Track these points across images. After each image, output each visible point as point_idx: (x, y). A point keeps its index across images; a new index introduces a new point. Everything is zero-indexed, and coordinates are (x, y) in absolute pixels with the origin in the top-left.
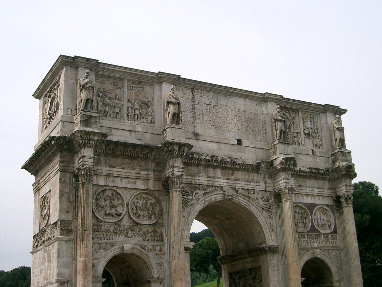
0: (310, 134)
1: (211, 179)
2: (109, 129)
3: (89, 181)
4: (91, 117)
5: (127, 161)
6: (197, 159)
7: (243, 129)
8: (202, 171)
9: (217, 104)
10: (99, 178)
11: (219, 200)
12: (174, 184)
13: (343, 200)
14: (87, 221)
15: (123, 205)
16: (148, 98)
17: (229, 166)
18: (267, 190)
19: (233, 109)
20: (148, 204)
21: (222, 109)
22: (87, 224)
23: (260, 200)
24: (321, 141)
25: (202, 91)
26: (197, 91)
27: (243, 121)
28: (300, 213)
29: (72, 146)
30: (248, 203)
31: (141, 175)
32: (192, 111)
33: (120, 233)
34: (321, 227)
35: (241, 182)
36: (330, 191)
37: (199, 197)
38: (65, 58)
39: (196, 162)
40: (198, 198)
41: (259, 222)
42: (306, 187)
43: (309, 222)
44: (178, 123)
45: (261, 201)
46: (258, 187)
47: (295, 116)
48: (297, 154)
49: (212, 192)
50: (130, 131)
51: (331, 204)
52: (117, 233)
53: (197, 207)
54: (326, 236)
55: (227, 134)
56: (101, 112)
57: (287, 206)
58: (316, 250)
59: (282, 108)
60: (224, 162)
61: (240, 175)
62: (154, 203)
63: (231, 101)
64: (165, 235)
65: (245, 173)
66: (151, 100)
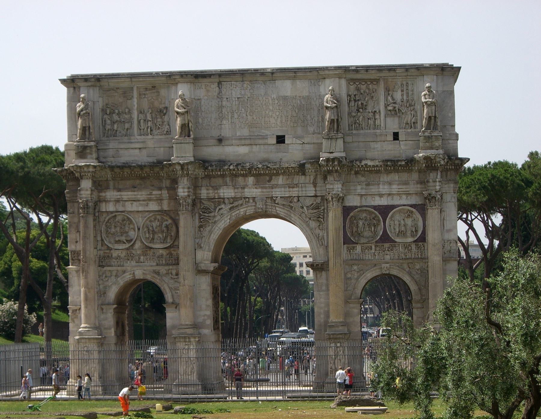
0: (396, 110)
1: (240, 190)
2: (116, 149)
4: (85, 148)
5: (138, 182)
8: (228, 181)
9: (252, 96)
10: (107, 204)
16: (164, 103)
17: (262, 172)
19: (275, 97)
20: (163, 226)
25: (233, 83)
27: (288, 110)
30: (289, 213)
33: (132, 260)
36: (419, 186)
39: (219, 173)
40: (222, 214)
42: (379, 184)
45: (307, 212)
46: (304, 192)
49: (242, 205)
50: (140, 148)
51: (420, 203)
52: (128, 259)
53: (221, 224)
54: (407, 246)
60: (253, 169)
61: (280, 180)
66: (168, 106)
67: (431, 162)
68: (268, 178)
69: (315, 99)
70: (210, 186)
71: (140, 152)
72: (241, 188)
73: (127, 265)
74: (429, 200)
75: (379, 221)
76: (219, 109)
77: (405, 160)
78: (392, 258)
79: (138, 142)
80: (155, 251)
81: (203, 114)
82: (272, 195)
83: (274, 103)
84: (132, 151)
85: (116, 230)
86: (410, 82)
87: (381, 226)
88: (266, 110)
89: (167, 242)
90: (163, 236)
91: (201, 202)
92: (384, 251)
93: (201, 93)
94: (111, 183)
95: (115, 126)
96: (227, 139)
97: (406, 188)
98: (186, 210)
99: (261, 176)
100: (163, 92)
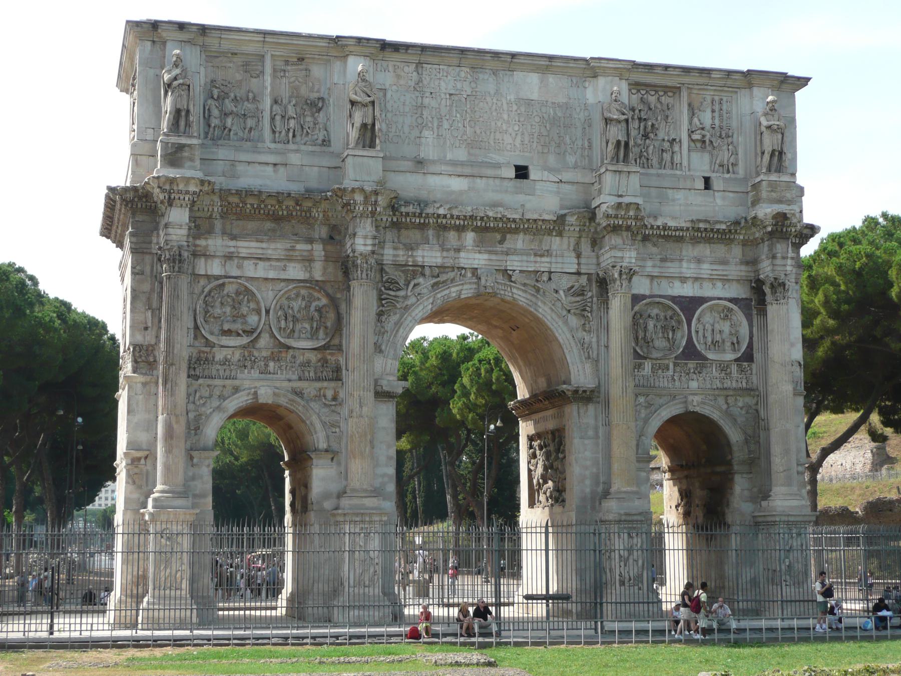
0: (704, 142)
1: (452, 253)
2: (231, 163)
3: (179, 272)
4: (181, 147)
5: (268, 225)
6: (417, 214)
7: (535, 144)
8: (431, 237)
9: (474, 93)
10: (209, 262)
11: (466, 296)
12: (357, 271)
13: (767, 289)
14: (173, 347)
15: (258, 312)
16: (318, 91)
17: (492, 225)
18: (583, 271)
20: (312, 309)
21: (487, 103)
22: (173, 353)
23: (561, 292)
24: (733, 156)
25: (441, 67)
26: (429, 66)
28: (662, 317)
29: (154, 202)
30: (534, 299)
31: (297, 253)
32: (415, 111)
33: (252, 368)
34: (712, 347)
35: (520, 256)
36: (743, 268)
37: (422, 292)
38: (137, 26)
39: (418, 221)
40: (419, 294)
41: (557, 340)
42: (681, 260)
43: (683, 337)
44: (372, 145)
46: (560, 266)
47: (672, 102)
48: (664, 190)
49: (453, 280)
50: (275, 165)
51: (744, 296)
53: (417, 311)
54: (724, 367)
55: (494, 156)
56: (216, 129)
57: (618, 306)
58: (690, 398)
59: (636, 86)
61: (520, 242)
62: (324, 306)
63: (509, 82)
64: (344, 368)
65: (532, 237)
66: (326, 96)
67: (783, 225)
68: (498, 236)
69: (578, 110)
70: (399, 242)
71: (274, 171)
72: (454, 249)
73: (243, 376)
74: (772, 286)
75: (679, 322)
76: (417, 109)
77: (726, 223)
78: (701, 386)
79: (272, 153)
80: (297, 353)
81: (389, 115)
82: (506, 266)
83: (510, 109)
84: (259, 168)
85: (224, 310)
86: (725, 99)
87: (683, 331)
88: (498, 120)
89: (317, 339)
90: (312, 328)
91: (382, 270)
92: (688, 374)
93: (385, 78)
94: (218, 224)
95: (229, 121)
96: (433, 162)
97: (723, 270)
98: (367, 279)
99: (488, 232)
100: (317, 71)
